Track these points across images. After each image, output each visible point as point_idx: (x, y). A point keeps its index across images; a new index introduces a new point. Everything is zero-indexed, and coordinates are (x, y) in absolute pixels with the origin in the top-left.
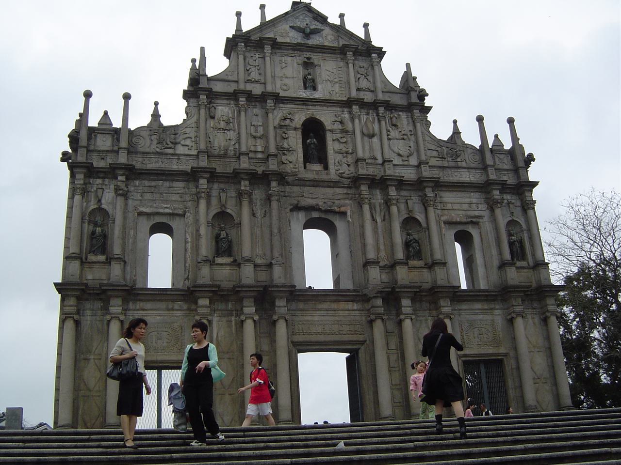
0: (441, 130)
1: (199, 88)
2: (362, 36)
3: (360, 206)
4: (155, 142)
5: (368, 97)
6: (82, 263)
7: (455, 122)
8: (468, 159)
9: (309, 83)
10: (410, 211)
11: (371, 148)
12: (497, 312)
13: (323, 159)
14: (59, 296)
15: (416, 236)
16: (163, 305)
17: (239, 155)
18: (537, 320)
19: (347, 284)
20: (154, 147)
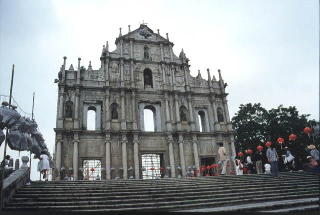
0: (194, 74)
2: (166, 38)
3: (165, 101)
5: (168, 61)
6: (64, 122)
7: (199, 71)
9: (146, 55)
10: (183, 104)
12: (213, 141)
13: (151, 84)
14: (55, 133)
15: (185, 113)
16: (93, 137)
17: (120, 82)
18: (227, 144)
19: (160, 130)
20: (90, 79)
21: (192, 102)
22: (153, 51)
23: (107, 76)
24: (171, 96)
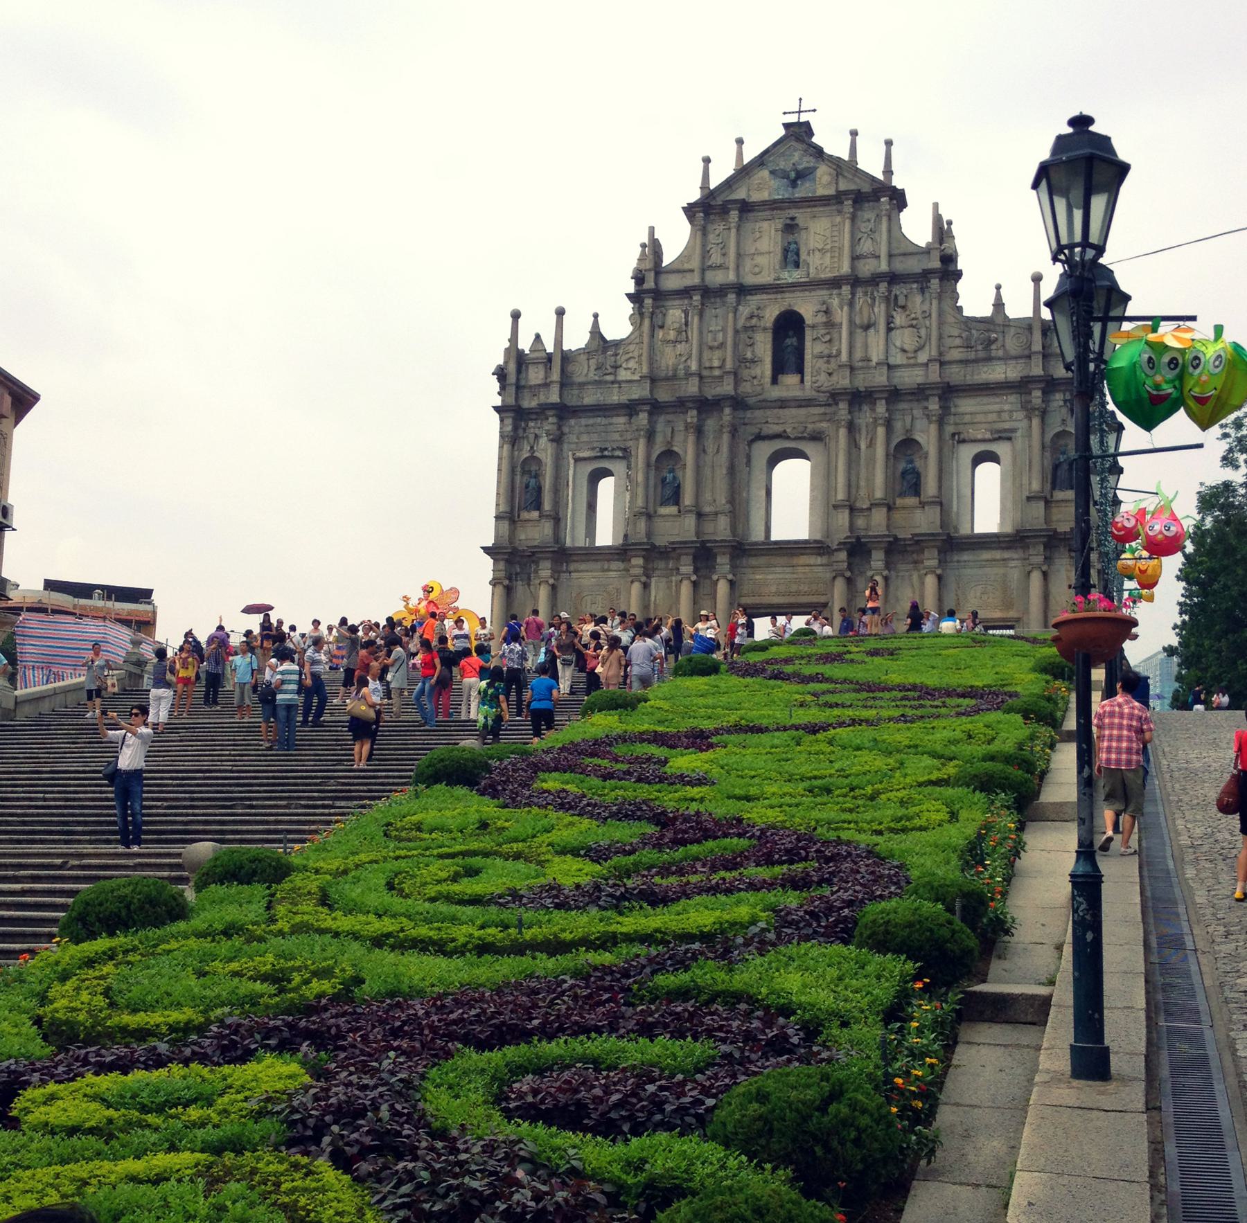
0: (974, 299)
4: (593, 368)
7: (998, 287)
8: (1012, 344)
9: (791, 257)
11: (866, 346)
12: (1013, 564)
13: (800, 370)
15: (918, 464)
16: (598, 565)
20: (593, 376)
21: (941, 422)
23: (645, 358)
24: (865, 408)
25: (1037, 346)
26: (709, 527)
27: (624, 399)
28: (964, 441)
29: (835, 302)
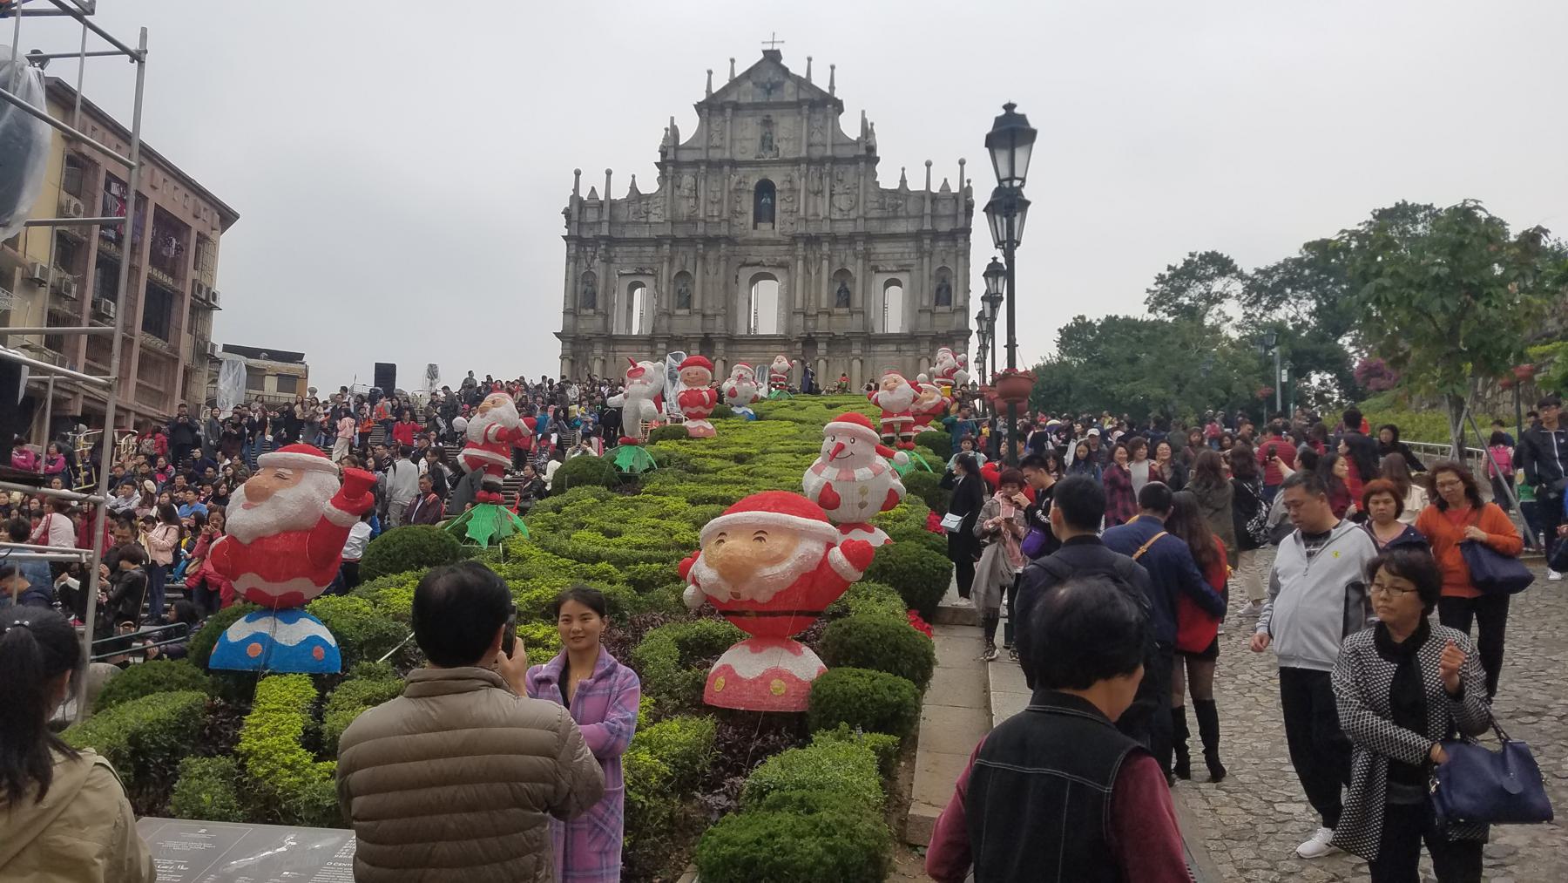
0: (887, 178)
1: (672, 159)
8: (912, 207)
9: (767, 143)
11: (815, 206)
13: (773, 221)
22: (786, 126)
25: (928, 210)
26: (709, 324)
27: (653, 235)
28: (878, 271)
29: (796, 175)
